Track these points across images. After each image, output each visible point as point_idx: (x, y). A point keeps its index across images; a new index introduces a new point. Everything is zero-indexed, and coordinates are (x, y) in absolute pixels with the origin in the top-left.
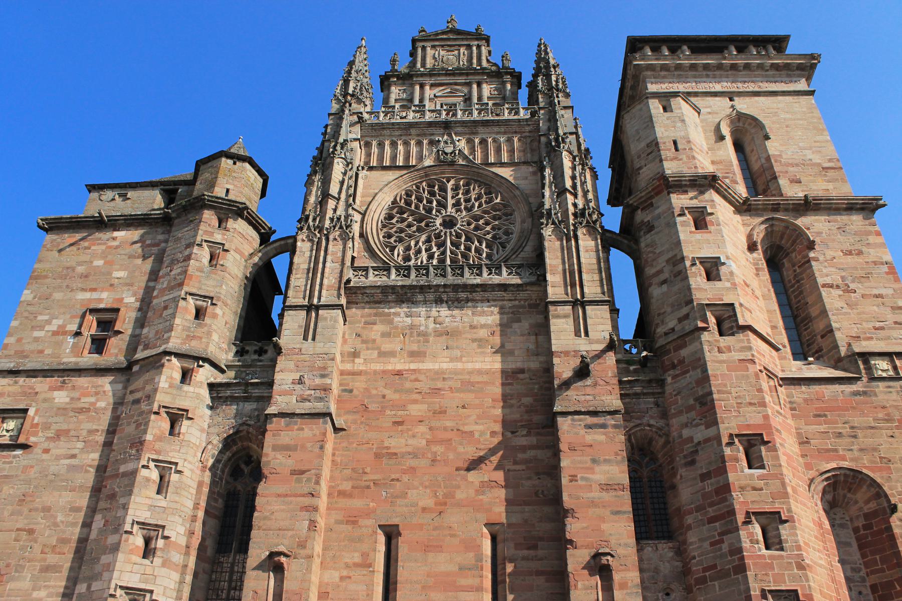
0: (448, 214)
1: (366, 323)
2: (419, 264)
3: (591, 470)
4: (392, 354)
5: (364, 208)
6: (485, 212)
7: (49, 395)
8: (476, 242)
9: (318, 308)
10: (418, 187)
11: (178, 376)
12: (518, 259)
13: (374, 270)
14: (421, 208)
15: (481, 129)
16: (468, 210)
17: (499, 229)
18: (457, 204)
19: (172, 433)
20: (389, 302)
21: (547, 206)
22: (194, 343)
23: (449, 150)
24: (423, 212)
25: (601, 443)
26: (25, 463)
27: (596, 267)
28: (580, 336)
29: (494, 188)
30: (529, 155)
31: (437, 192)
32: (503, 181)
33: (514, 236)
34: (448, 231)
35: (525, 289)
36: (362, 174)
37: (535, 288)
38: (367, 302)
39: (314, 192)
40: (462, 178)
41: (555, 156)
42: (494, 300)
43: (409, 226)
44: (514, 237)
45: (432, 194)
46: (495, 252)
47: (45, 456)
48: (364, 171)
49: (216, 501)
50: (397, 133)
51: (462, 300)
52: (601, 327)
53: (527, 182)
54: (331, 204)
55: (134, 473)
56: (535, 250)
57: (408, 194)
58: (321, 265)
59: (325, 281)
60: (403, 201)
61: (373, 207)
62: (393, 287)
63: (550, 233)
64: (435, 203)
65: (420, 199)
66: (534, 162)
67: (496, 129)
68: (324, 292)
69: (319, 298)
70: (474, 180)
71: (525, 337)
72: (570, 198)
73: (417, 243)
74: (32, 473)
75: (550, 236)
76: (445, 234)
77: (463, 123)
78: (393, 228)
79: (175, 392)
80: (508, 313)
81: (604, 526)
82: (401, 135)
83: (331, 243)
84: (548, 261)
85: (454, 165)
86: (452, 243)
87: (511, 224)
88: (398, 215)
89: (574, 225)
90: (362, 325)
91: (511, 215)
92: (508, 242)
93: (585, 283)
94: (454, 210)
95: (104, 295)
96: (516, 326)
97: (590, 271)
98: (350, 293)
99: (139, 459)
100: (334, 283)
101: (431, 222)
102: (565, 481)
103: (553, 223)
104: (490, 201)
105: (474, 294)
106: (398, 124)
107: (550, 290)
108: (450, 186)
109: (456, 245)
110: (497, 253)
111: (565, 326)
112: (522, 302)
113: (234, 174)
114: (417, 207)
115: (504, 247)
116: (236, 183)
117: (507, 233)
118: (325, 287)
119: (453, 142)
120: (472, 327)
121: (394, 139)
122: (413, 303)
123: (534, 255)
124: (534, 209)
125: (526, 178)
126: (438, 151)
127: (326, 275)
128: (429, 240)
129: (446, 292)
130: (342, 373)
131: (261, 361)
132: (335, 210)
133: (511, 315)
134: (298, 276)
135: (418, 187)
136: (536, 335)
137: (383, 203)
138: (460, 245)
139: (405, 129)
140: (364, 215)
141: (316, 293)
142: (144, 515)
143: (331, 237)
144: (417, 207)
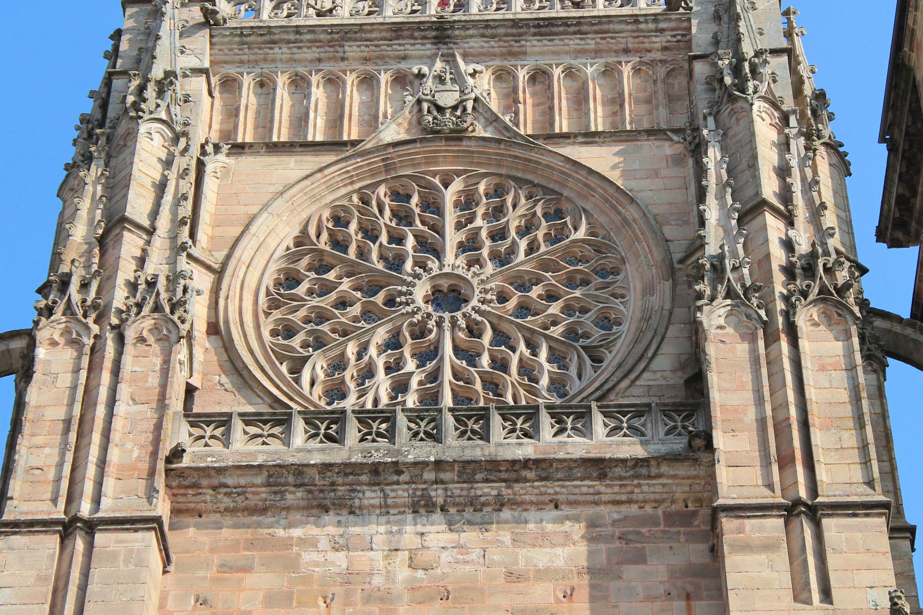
0: (447, 270)
1: (225, 567)
2: (369, 406)
5: (220, 255)
6: (546, 265)
8: (522, 347)
9: (91, 527)
10: (365, 201)
12: (634, 391)
13: (247, 423)
14: (374, 256)
15: (533, 44)
16: (502, 259)
17: (584, 311)
18: (470, 246)
20: (288, 509)
21: (712, 249)
23: (448, 99)
24: (380, 266)
27: (847, 410)
28: (809, 602)
29: (568, 199)
30: (663, 112)
31: (417, 211)
32: (593, 181)
33: (624, 328)
34: (447, 315)
35: (654, 471)
36: (214, 163)
37: (683, 470)
38: (227, 510)
39: (83, 213)
40: (485, 175)
41: (733, 112)
42: (572, 503)
43: (343, 304)
44: (626, 332)
45: (403, 217)
46: (573, 371)
48: (221, 157)
51: (484, 504)
52: (866, 578)
53: (657, 183)
54: (131, 243)
56: (682, 367)
57: (340, 220)
58: (101, 411)
59: (114, 454)
60: (325, 236)
61: (244, 252)
62: (299, 470)
63: (722, 321)
64: (410, 242)
65: (370, 234)
66: (676, 131)
67: (574, 42)
68: (109, 484)
69: (97, 501)
70: (515, 179)
71: (658, 604)
72: (774, 226)
73: (363, 349)
75: (721, 327)
76: (439, 324)
77: (486, 27)
78: (295, 310)
80: (608, 539)
82: (319, 60)
83: (129, 349)
84: (716, 396)
85: (460, 139)
86: (457, 349)
87: (614, 295)
88: (313, 275)
89: (786, 299)
90: (212, 573)
91: (615, 272)
92: (609, 345)
93: (819, 455)
94: (461, 261)
96: (631, 572)
98: (180, 487)
100: (138, 459)
101: (401, 294)
103: (730, 294)
105: (517, 487)
106: (312, 29)
107: (723, 474)
108: (450, 195)
109: (468, 355)
110: (580, 377)
111: (767, 573)
112: (648, 509)
114: (362, 253)
115: (597, 360)
118: (110, 470)
119: (458, 78)
120: (513, 576)
121: (301, 70)
122: (352, 513)
123: (678, 379)
124: (677, 256)
125: (656, 174)
126: (419, 102)
127: (115, 436)
128: (394, 343)
129: (442, 482)
132: (141, 262)
133: (617, 544)
134: (39, 440)
135: (365, 201)
136: (688, 597)
137: (272, 243)
138: (479, 355)
139: (330, 43)
140: (219, 273)
141: (89, 487)
143: (130, 334)
144: (362, 253)
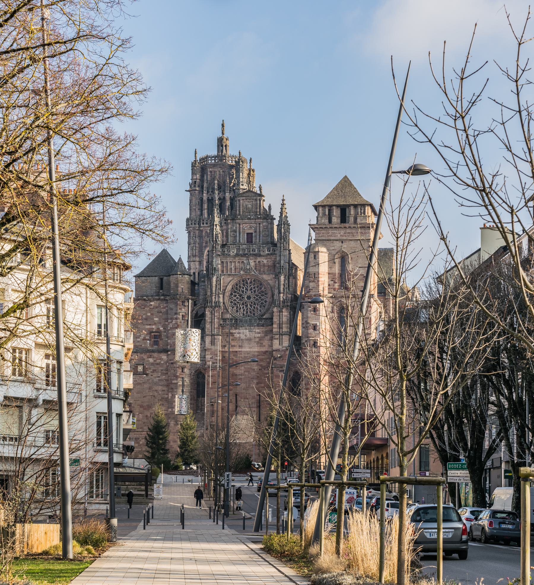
4: (234, 346)
6: (259, 293)
7: (147, 359)
16: (255, 291)
18: (251, 289)
55: (177, 383)
57: (237, 285)
74: (150, 381)
95: (154, 327)
104: (261, 288)
108: (249, 282)
109: (251, 306)
117: (266, 302)
128: (243, 304)
130: (222, 352)
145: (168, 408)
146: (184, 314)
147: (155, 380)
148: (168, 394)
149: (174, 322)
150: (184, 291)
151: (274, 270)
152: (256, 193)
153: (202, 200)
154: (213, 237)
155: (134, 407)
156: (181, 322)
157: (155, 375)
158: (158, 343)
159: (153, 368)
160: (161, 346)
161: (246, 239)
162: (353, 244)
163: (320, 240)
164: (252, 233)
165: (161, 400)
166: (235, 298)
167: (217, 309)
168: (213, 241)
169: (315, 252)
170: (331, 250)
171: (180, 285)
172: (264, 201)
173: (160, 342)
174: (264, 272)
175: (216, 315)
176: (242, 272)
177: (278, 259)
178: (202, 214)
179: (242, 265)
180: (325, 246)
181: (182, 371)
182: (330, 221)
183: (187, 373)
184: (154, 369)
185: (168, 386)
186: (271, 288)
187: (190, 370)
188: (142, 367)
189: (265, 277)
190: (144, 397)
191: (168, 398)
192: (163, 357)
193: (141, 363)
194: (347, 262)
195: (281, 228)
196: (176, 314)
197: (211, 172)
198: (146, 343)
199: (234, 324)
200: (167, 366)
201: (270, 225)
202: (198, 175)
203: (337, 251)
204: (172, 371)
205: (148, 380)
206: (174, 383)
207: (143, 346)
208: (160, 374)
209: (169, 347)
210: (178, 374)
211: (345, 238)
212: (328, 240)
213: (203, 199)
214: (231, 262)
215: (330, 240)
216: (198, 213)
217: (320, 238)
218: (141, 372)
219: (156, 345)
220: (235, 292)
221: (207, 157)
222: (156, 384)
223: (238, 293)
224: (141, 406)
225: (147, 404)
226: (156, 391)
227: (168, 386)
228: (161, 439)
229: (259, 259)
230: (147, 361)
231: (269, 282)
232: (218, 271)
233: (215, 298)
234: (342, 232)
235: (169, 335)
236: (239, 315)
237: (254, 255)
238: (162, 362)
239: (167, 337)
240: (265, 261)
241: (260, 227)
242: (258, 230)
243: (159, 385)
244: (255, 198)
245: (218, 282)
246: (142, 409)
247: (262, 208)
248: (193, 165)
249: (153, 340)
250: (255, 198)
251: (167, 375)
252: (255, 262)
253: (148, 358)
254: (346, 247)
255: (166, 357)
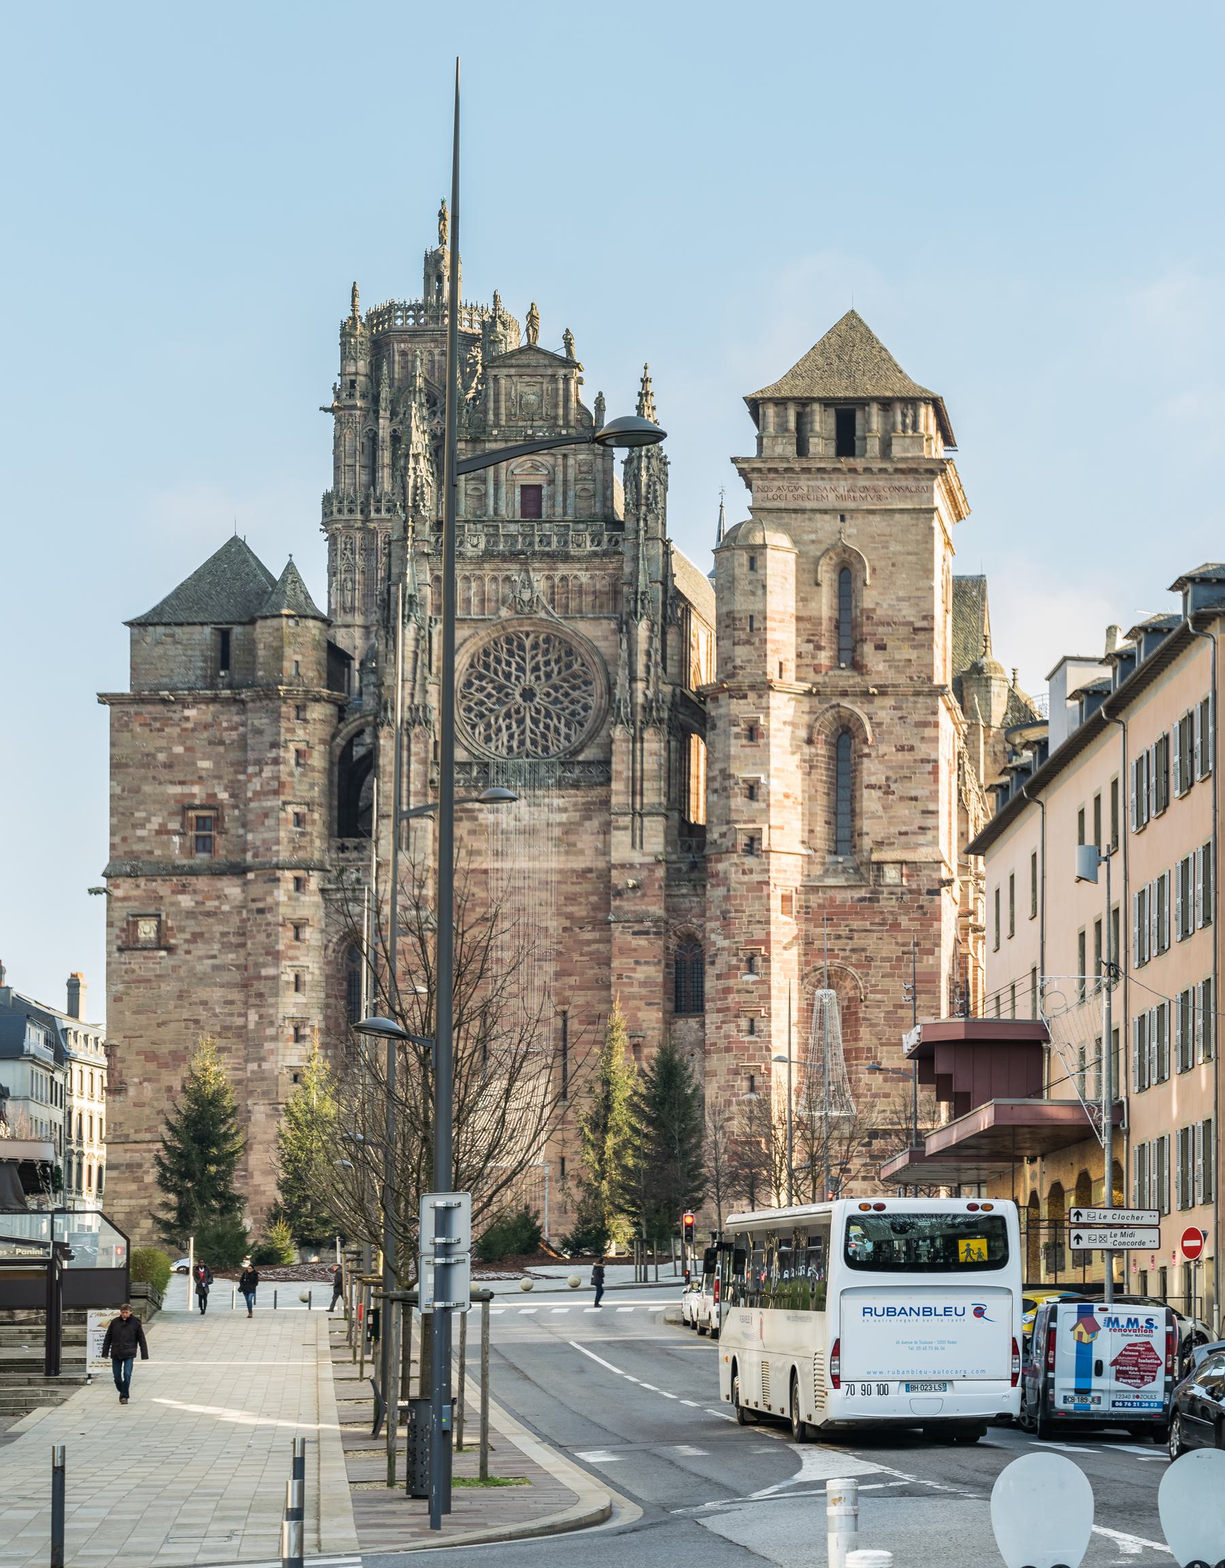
3: (634, 970)
11: (291, 886)
19: (297, 938)
22: (301, 854)
25: (643, 948)
26: (172, 963)
47: (188, 957)
49: (341, 984)
50: (469, 567)
55: (275, 978)
59: (412, 788)
67: (578, 566)
68: (412, 799)
69: (408, 804)
71: (593, 837)
74: (183, 972)
79: (293, 903)
81: (640, 1014)
83: (413, 741)
97: (653, 778)
99: (277, 965)
102: (613, 979)
113: (300, 640)
116: (303, 650)
125: (606, 639)
127: (412, 780)
131: (362, 860)
141: (404, 800)
142: (292, 1011)
145: (247, 1061)
146: (302, 746)
147: (199, 968)
148: (245, 1015)
149: (268, 772)
150: (302, 671)
151: (615, 606)
152: (553, 356)
153: (373, 437)
154: (405, 494)
155: (123, 1060)
156: (291, 774)
157: (200, 949)
158: (212, 844)
159: (192, 926)
160: (223, 852)
161: (518, 505)
162: (877, 524)
163: (770, 510)
164: (539, 487)
165: (220, 1035)
166: (480, 696)
167: (417, 729)
168: (404, 507)
169: (753, 547)
170: (804, 543)
171: (288, 651)
172: (580, 381)
173: (220, 841)
174: (580, 611)
175: (413, 748)
176: (504, 613)
177: (627, 569)
178: (373, 482)
179: (504, 590)
180: (786, 529)
181: (297, 938)
182: (802, 450)
183: (313, 943)
184: (198, 930)
185: (245, 986)
186: (605, 664)
187: (322, 931)
188: (154, 923)
189: (586, 629)
190: (159, 1025)
191: (245, 1027)
192: (228, 891)
193: (151, 910)
194: (859, 584)
195: (639, 469)
196: (275, 745)
197: (403, 354)
198: (166, 845)
199: (477, 780)
200: (243, 921)
201: (599, 461)
202: (361, 363)
203: (824, 547)
204: (262, 937)
205: (175, 968)
206: (267, 978)
207: (157, 852)
208: (216, 946)
209: (249, 856)
210: (281, 947)
211: (851, 505)
212: (795, 511)
213: (376, 434)
214: (466, 578)
215: (803, 511)
216: (363, 478)
217: (769, 505)
218: (150, 941)
219: (205, 850)
220: (481, 677)
221: (391, 308)
222: (202, 980)
223: (492, 681)
224: (150, 1056)
225: (173, 1047)
226: (204, 1003)
227: (245, 986)
228: (217, 1161)
229: (563, 570)
230: (172, 904)
231: (596, 643)
232: (423, 606)
233: (412, 695)
234: (843, 485)
235: (251, 817)
236: (496, 751)
237: (548, 554)
238: (226, 908)
239: (244, 825)
240: (584, 577)
241: (565, 467)
242: (560, 477)
243: (215, 984)
244: (549, 371)
245: (424, 644)
246: (152, 1066)
247: (573, 404)
248: (346, 332)
249: (192, 833)
250: (549, 371)
251: (242, 952)
252: (549, 578)
253: (174, 892)
254: (853, 534)
255: (238, 890)
